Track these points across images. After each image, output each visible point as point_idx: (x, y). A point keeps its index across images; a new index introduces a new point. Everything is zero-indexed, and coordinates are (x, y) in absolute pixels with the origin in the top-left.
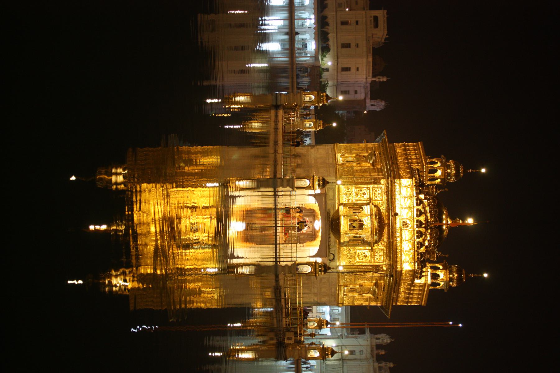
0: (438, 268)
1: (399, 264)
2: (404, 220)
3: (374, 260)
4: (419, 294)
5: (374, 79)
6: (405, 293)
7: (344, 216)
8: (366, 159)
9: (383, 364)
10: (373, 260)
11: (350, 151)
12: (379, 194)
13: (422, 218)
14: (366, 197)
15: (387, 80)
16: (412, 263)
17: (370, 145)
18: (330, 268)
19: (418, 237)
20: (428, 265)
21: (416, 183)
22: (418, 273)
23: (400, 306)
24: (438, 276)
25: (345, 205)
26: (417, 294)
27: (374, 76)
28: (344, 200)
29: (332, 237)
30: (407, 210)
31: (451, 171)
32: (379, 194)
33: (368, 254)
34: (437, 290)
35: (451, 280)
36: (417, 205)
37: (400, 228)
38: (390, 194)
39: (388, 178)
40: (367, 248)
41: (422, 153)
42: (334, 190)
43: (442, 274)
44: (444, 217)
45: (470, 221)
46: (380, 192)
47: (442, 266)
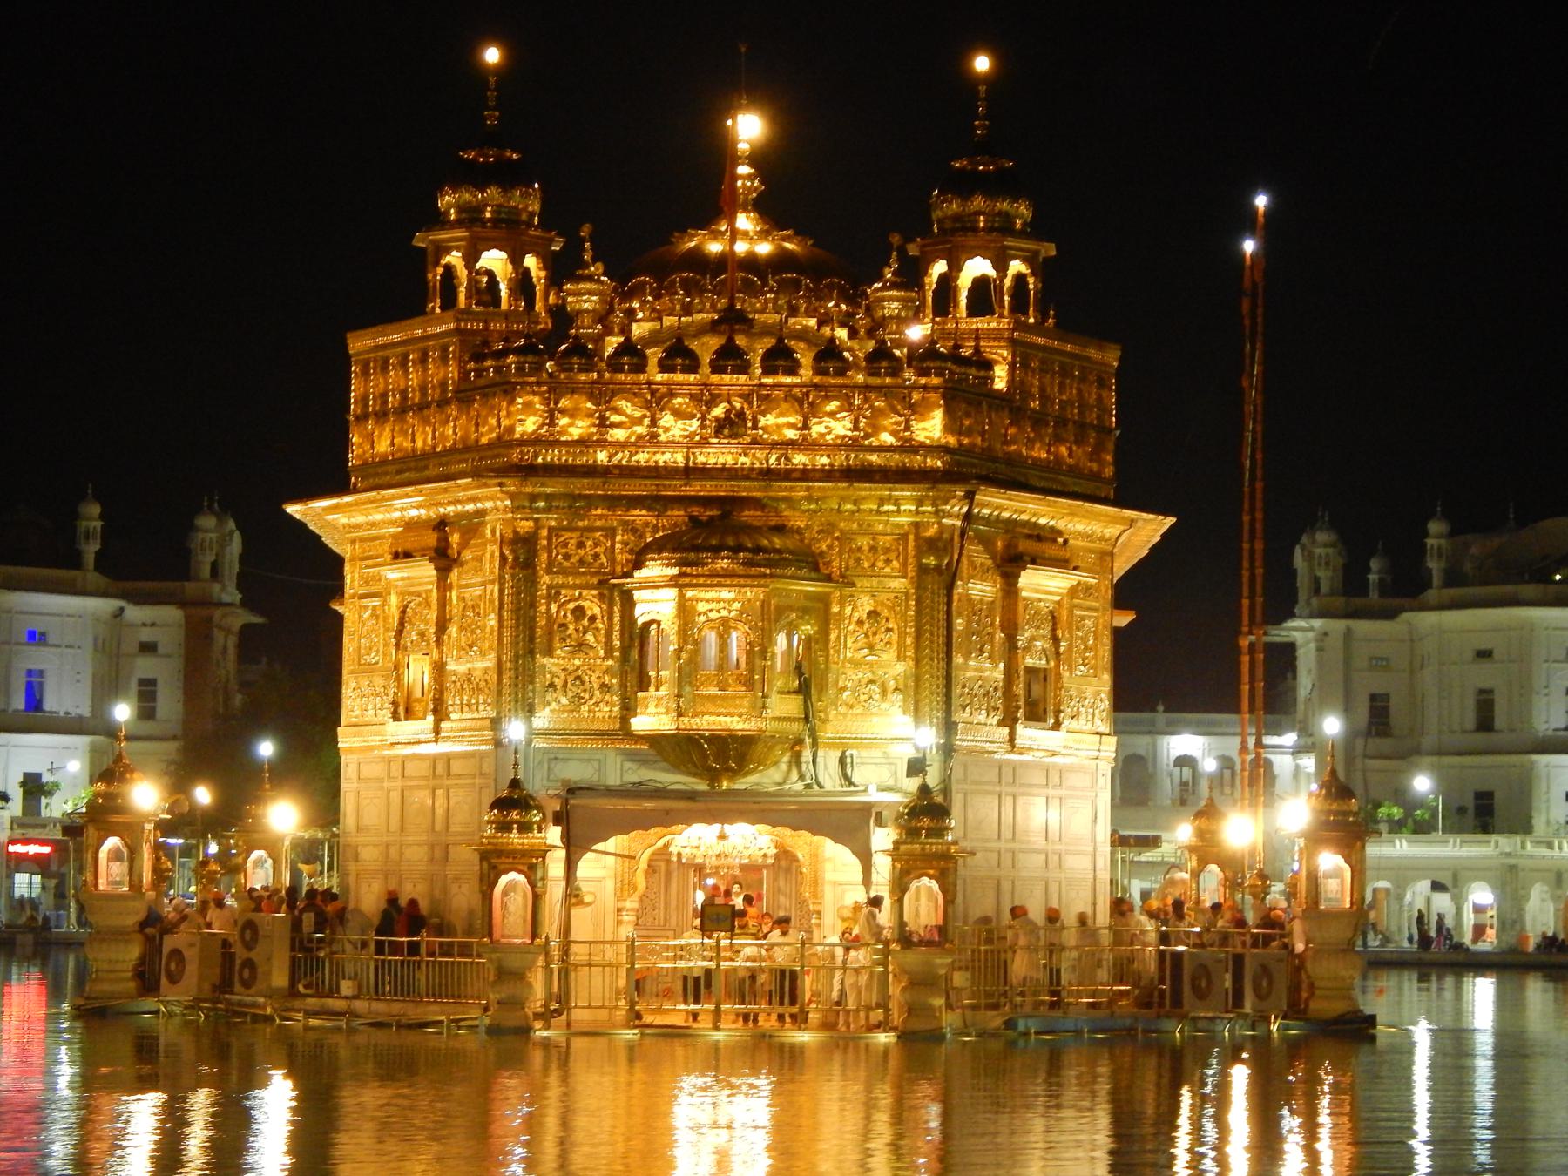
0: (947, 283)
2: (710, 431)
4: (1065, 372)
6: (1058, 439)
7: (680, 715)
9: (1434, 565)
12: (581, 545)
14: (593, 608)
15: (98, 498)
19: (793, 370)
23: (1117, 462)
24: (981, 284)
25: (628, 709)
26: (1062, 386)
27: (75, 562)
30: (667, 419)
32: (581, 545)
40: (835, 609)
46: (572, 538)
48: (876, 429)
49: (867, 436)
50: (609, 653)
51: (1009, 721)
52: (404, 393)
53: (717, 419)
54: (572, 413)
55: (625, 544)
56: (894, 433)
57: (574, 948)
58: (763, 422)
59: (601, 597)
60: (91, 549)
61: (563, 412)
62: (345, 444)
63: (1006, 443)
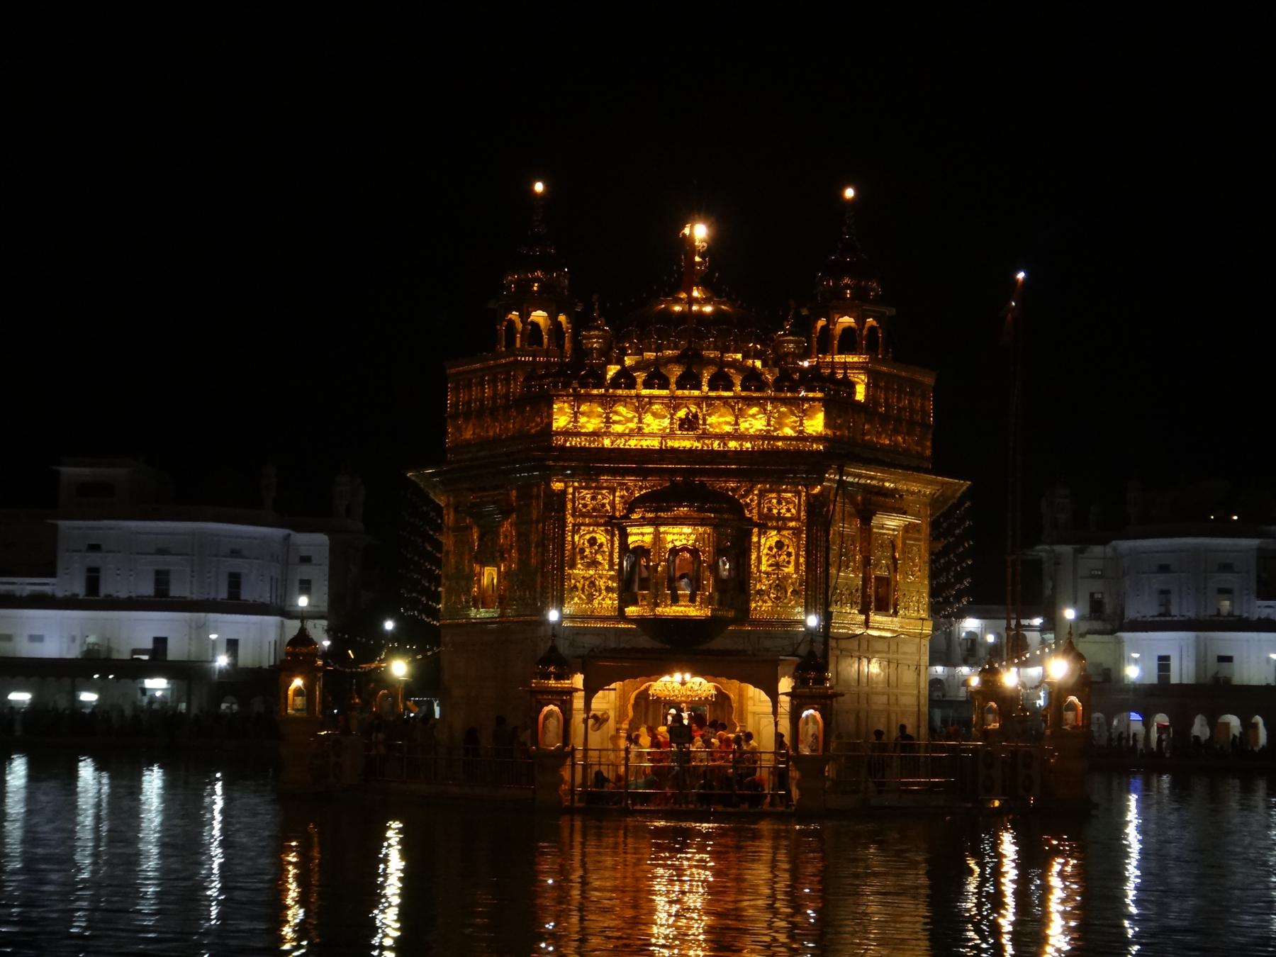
3: (791, 519)
6: (896, 432)
7: (657, 605)
8: (489, 533)
10: (793, 524)
13: (676, 371)
14: (602, 538)
18: (811, 654)
19: (729, 387)
22: (837, 392)
23: (934, 447)
24: (848, 331)
29: (719, 643)
30: (648, 418)
31: (537, 280)
32: (593, 498)
33: (773, 538)
36: (631, 384)
37: (698, 438)
38: (596, 463)
39: (549, 467)
40: (755, 539)
44: (677, 308)
46: (587, 494)
47: (819, 318)
48: (781, 425)
49: (776, 429)
50: (611, 568)
51: (864, 611)
52: (482, 401)
53: (681, 419)
54: (588, 415)
55: (622, 497)
56: (793, 428)
57: (591, 753)
58: (710, 420)
59: (607, 531)
61: (583, 414)
63: (864, 434)
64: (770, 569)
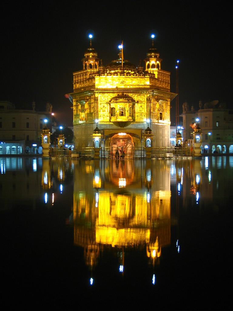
1: (146, 87)
5: (34, 109)
8: (83, 106)
11: (77, 115)
16: (146, 79)
17: (74, 104)
18: (148, 128)
20: (147, 70)
21: (97, 76)
22: (152, 76)
23: (170, 87)
27: (32, 109)
28: (107, 119)
31: (91, 55)
32: (104, 98)
33: (140, 105)
34: (161, 65)
35: (155, 57)
38: (104, 91)
39: (95, 92)
41: (80, 73)
42: (102, 125)
43: (153, 62)
45: (121, 47)
46: (103, 97)
48: (141, 83)
50: (108, 112)
56: (143, 83)
60: (34, 108)
62: (73, 87)
64: (139, 111)
